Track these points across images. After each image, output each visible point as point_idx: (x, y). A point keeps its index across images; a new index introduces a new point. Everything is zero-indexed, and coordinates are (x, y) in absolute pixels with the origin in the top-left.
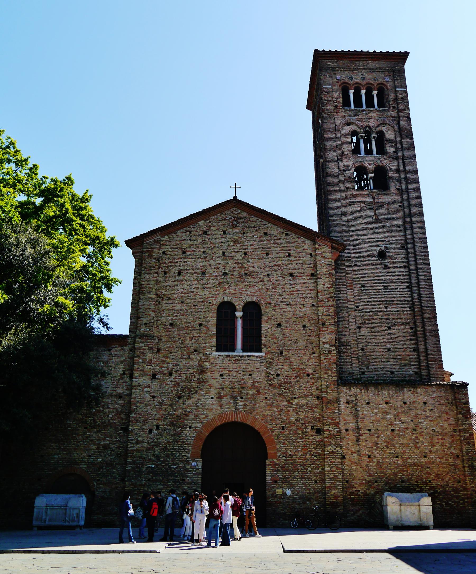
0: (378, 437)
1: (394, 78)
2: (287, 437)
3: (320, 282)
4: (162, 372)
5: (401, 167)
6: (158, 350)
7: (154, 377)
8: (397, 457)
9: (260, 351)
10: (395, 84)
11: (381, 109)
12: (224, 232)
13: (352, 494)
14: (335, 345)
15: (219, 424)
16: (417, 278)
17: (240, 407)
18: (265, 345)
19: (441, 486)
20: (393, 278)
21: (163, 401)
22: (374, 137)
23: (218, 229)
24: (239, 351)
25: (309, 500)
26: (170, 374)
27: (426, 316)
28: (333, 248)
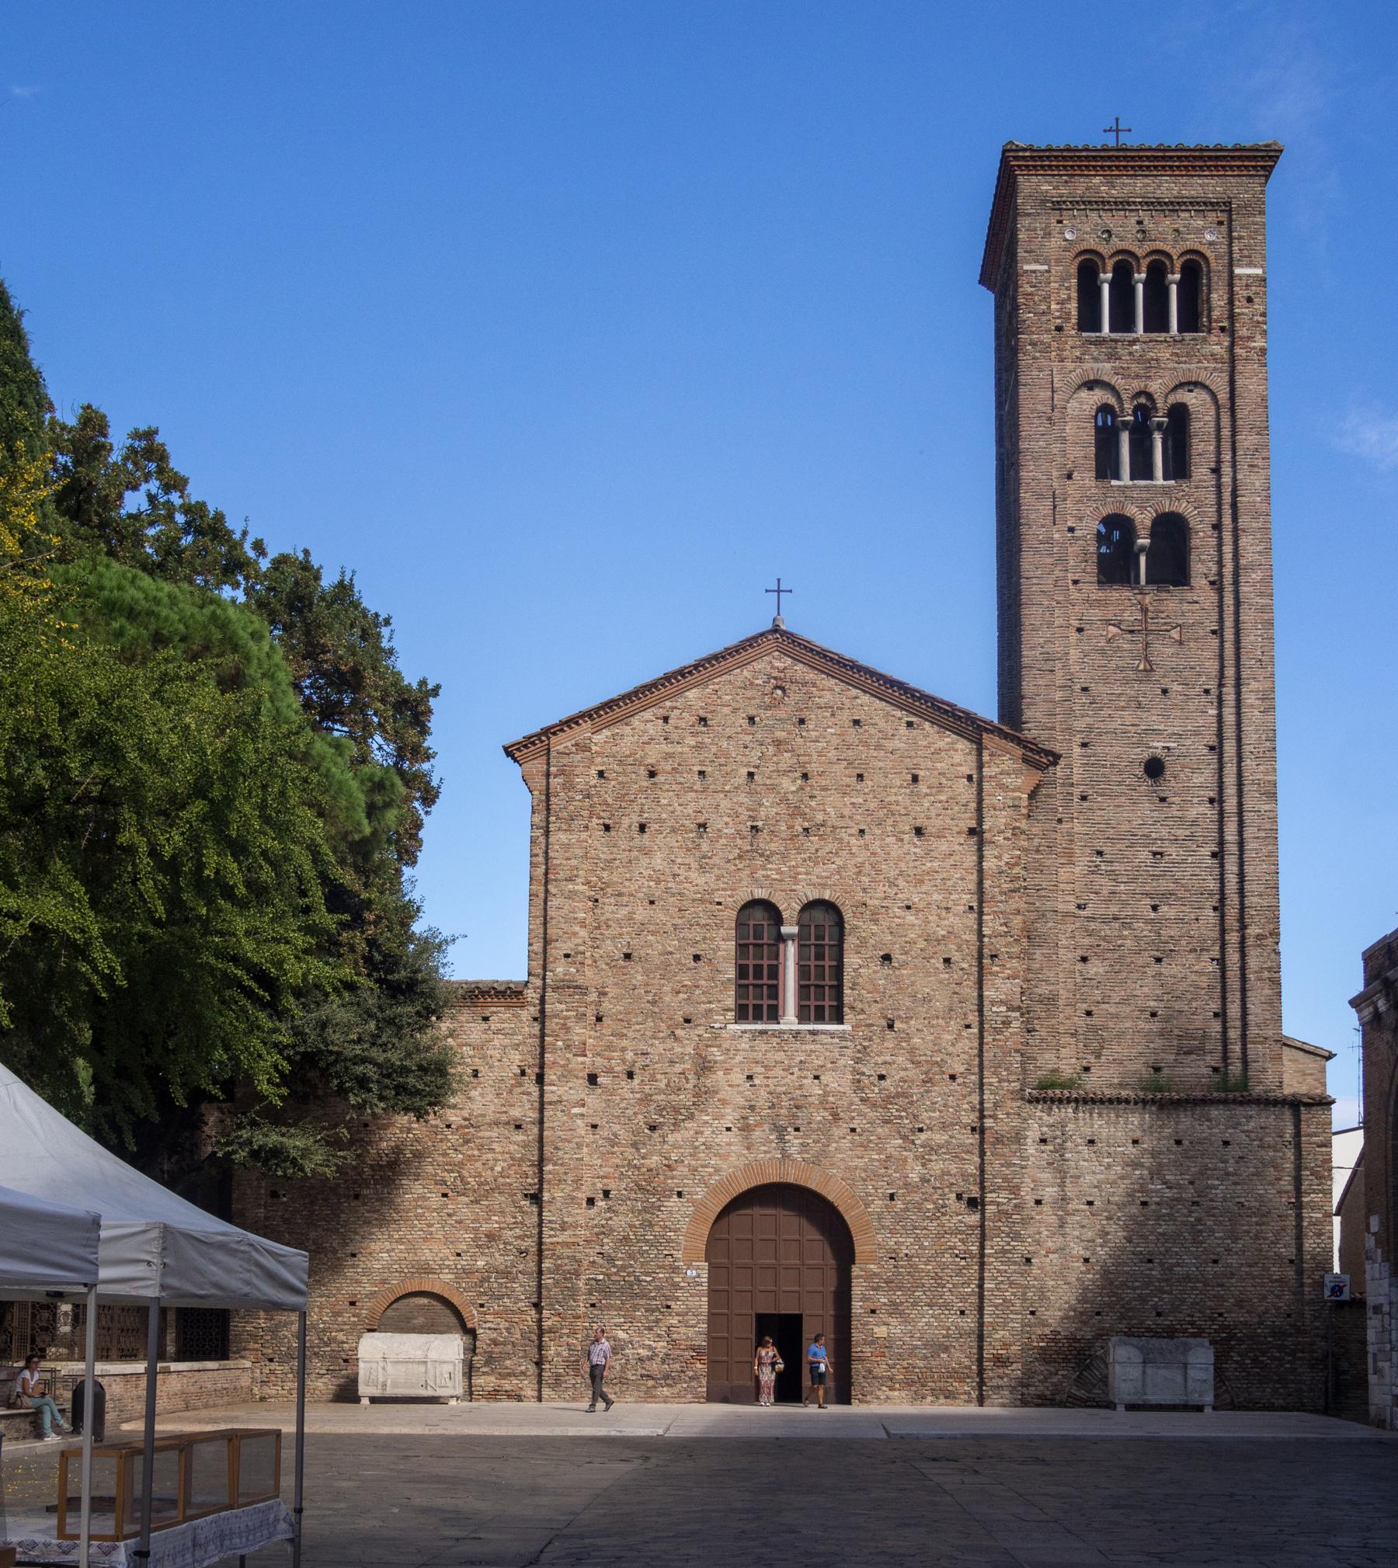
0: (1108, 1219)
1: (1230, 231)
2: (899, 1219)
3: (988, 851)
4: (610, 1071)
5: (1227, 520)
6: (599, 1019)
7: (592, 1079)
8: (1150, 1261)
9: (839, 1019)
10: (1231, 253)
11: (1188, 336)
12: (751, 719)
13: (1041, 1338)
14: (1019, 1008)
15: (745, 1187)
16: (1240, 833)
17: (793, 1150)
18: (852, 1008)
19: (1245, 1323)
20: (1179, 832)
21: (616, 1135)
22: (1160, 424)
23: (735, 710)
24: (790, 1020)
25: (946, 1349)
26: (630, 1075)
27: (1252, 931)
28: (1025, 760)
